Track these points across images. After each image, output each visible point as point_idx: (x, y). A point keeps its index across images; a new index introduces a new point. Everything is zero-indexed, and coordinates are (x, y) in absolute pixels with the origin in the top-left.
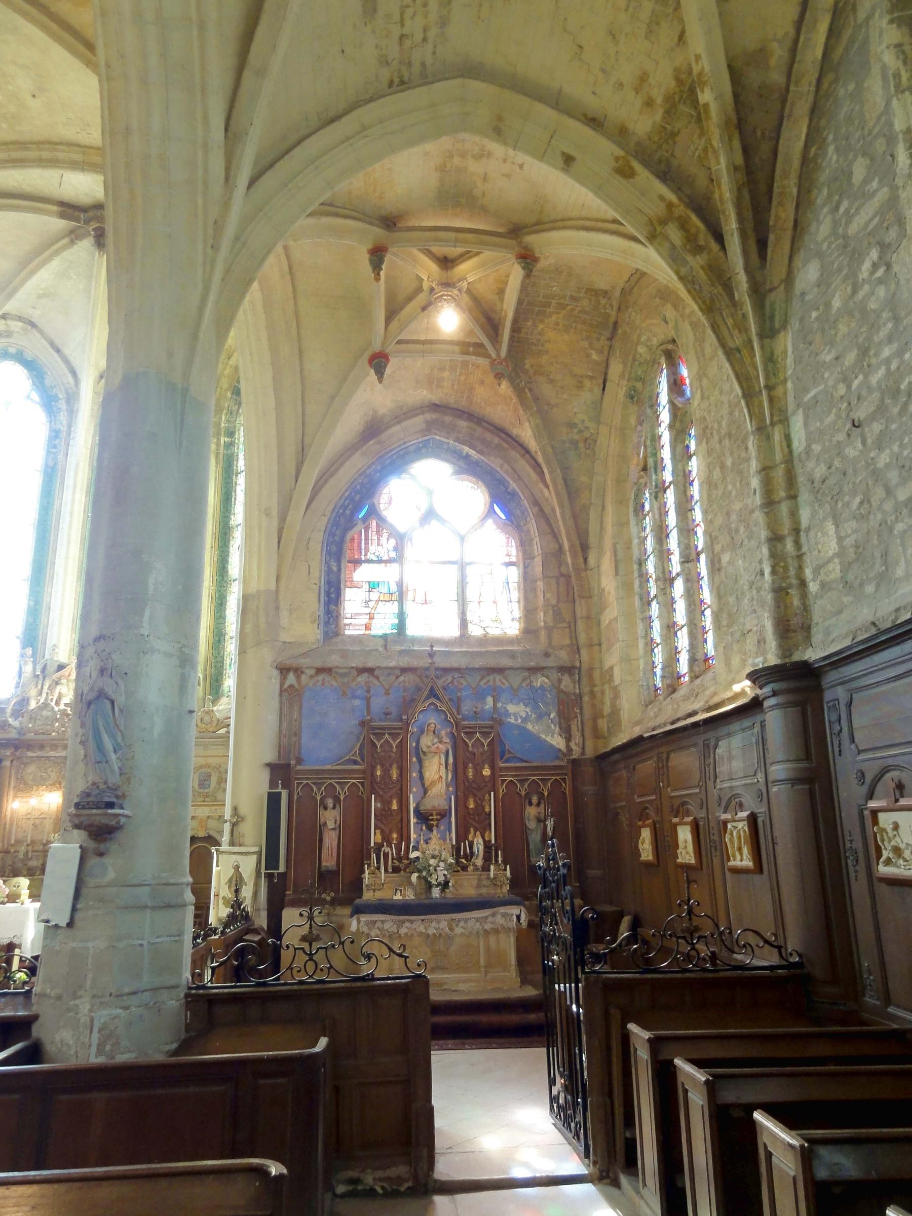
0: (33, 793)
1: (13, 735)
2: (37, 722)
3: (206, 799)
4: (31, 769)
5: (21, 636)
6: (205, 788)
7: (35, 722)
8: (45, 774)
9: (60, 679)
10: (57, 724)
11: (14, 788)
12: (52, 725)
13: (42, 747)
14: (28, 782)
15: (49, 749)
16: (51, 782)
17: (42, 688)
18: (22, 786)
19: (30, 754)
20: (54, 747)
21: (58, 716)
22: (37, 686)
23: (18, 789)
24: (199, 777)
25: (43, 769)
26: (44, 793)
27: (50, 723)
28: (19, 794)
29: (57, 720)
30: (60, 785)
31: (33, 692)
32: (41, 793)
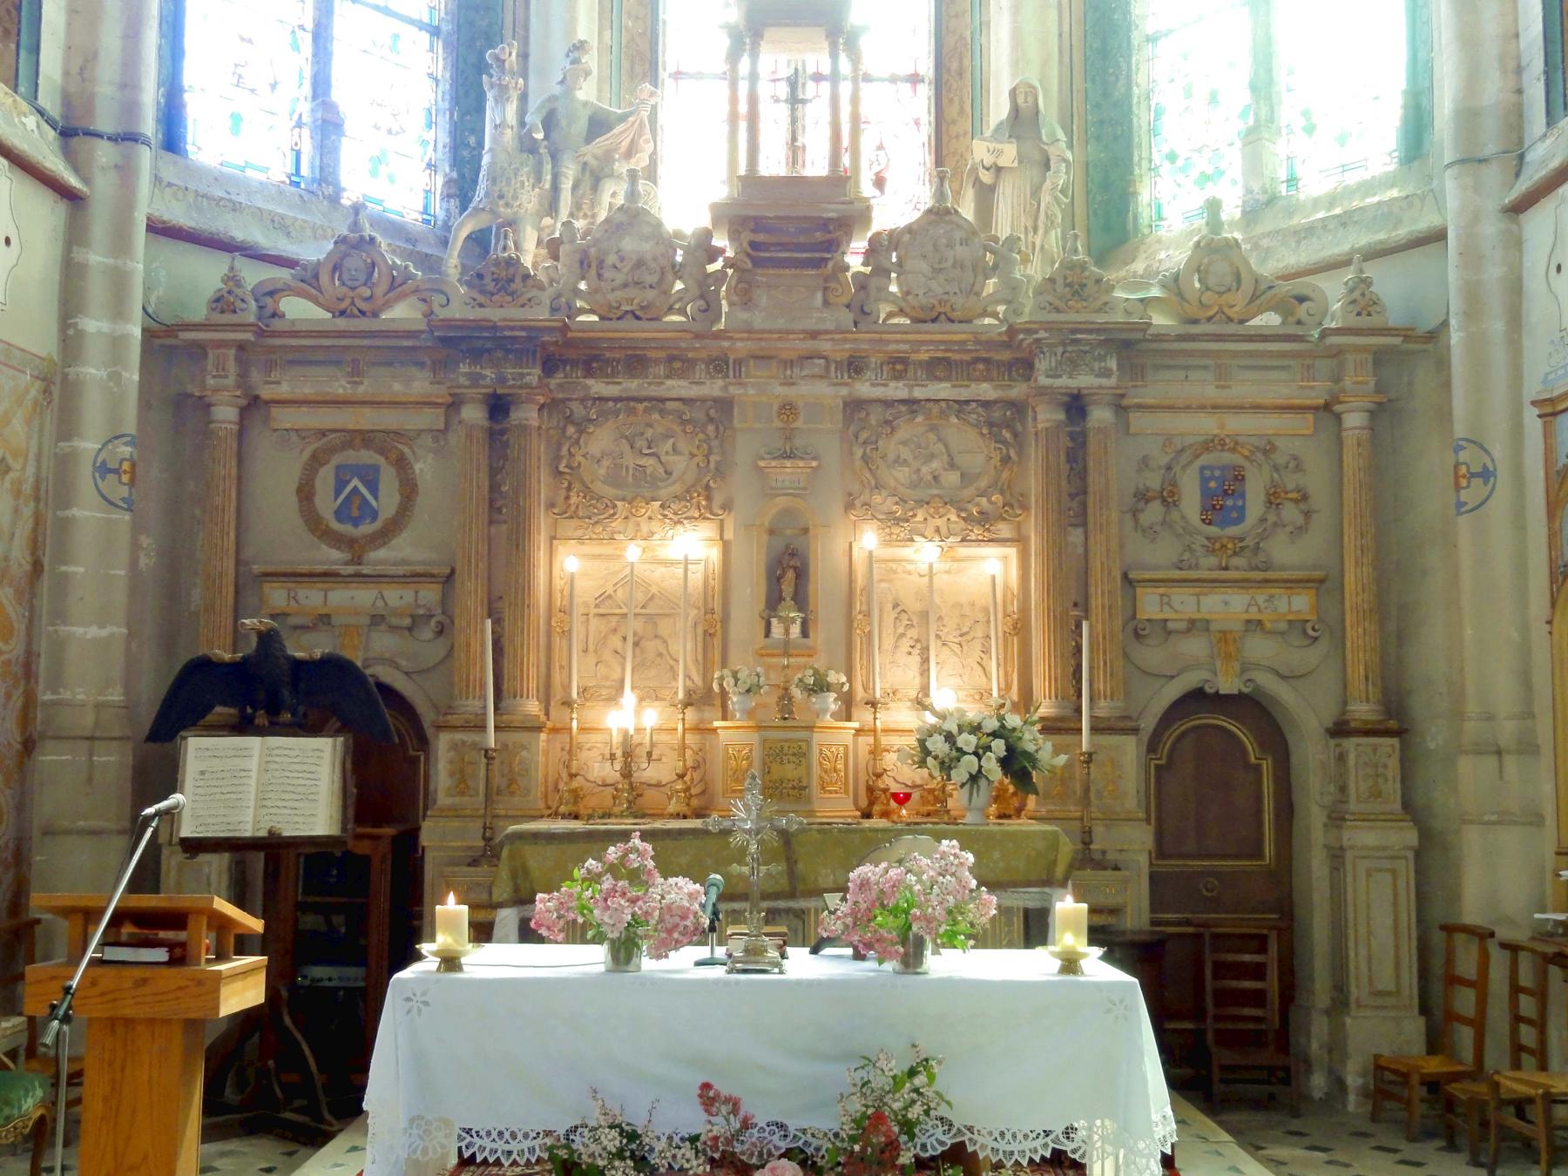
0: (616, 524)
1: (540, 314)
2: (607, 274)
3: (1236, 561)
4: (601, 440)
5: (446, 28)
6: (1224, 524)
7: (599, 276)
8: (651, 461)
9: (607, 158)
10: (679, 286)
11: (551, 505)
12: (662, 286)
13: (636, 362)
14: (600, 488)
15: (661, 370)
16: (677, 488)
17: (555, 188)
18: (574, 500)
19: (598, 387)
20: (679, 363)
21: (679, 259)
22: (539, 179)
23: (563, 510)
24: (1204, 481)
25: (641, 443)
26: (655, 526)
27: (653, 279)
28: (567, 527)
29: (678, 271)
30: (709, 498)
31: (529, 200)
32: (645, 528)
